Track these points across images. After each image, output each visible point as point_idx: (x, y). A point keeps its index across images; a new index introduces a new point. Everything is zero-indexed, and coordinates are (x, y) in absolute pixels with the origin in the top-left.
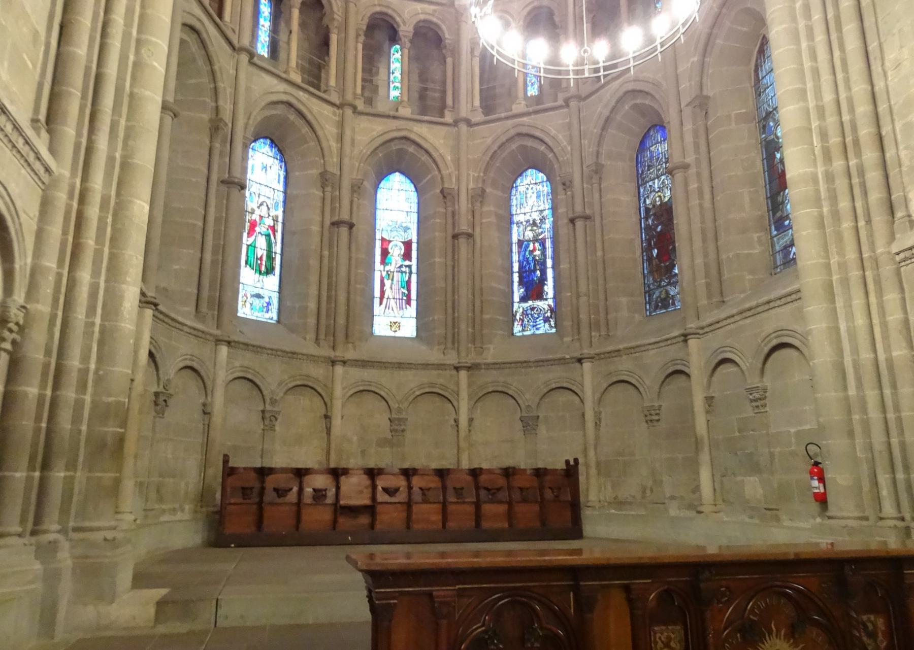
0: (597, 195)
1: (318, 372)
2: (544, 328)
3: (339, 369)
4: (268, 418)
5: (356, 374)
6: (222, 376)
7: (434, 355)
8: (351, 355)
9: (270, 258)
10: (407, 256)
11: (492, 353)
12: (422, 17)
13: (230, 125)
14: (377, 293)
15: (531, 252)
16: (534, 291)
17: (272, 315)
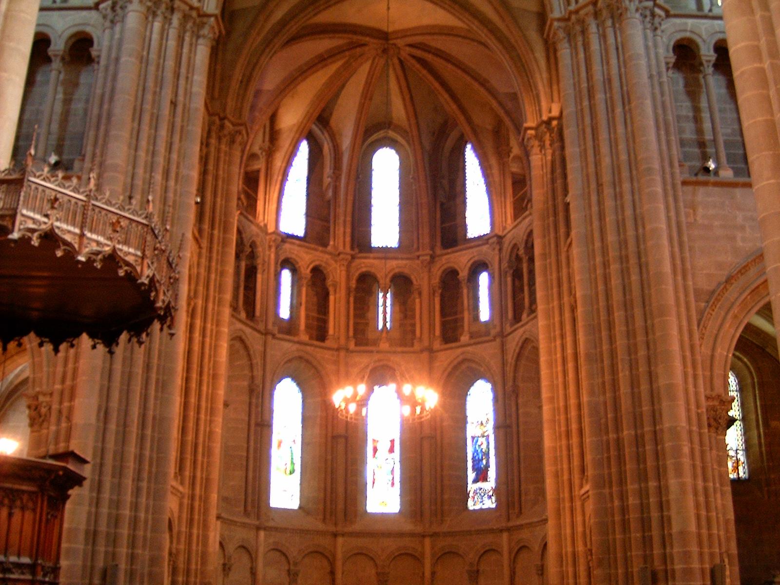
0: (514, 409)
1: (325, 542)
2: (490, 504)
6: (261, 550)
7: (408, 527)
8: (350, 529)
9: (293, 463)
10: (392, 450)
12: (397, 271)
13: (261, 386)
15: (480, 446)
16: (482, 476)
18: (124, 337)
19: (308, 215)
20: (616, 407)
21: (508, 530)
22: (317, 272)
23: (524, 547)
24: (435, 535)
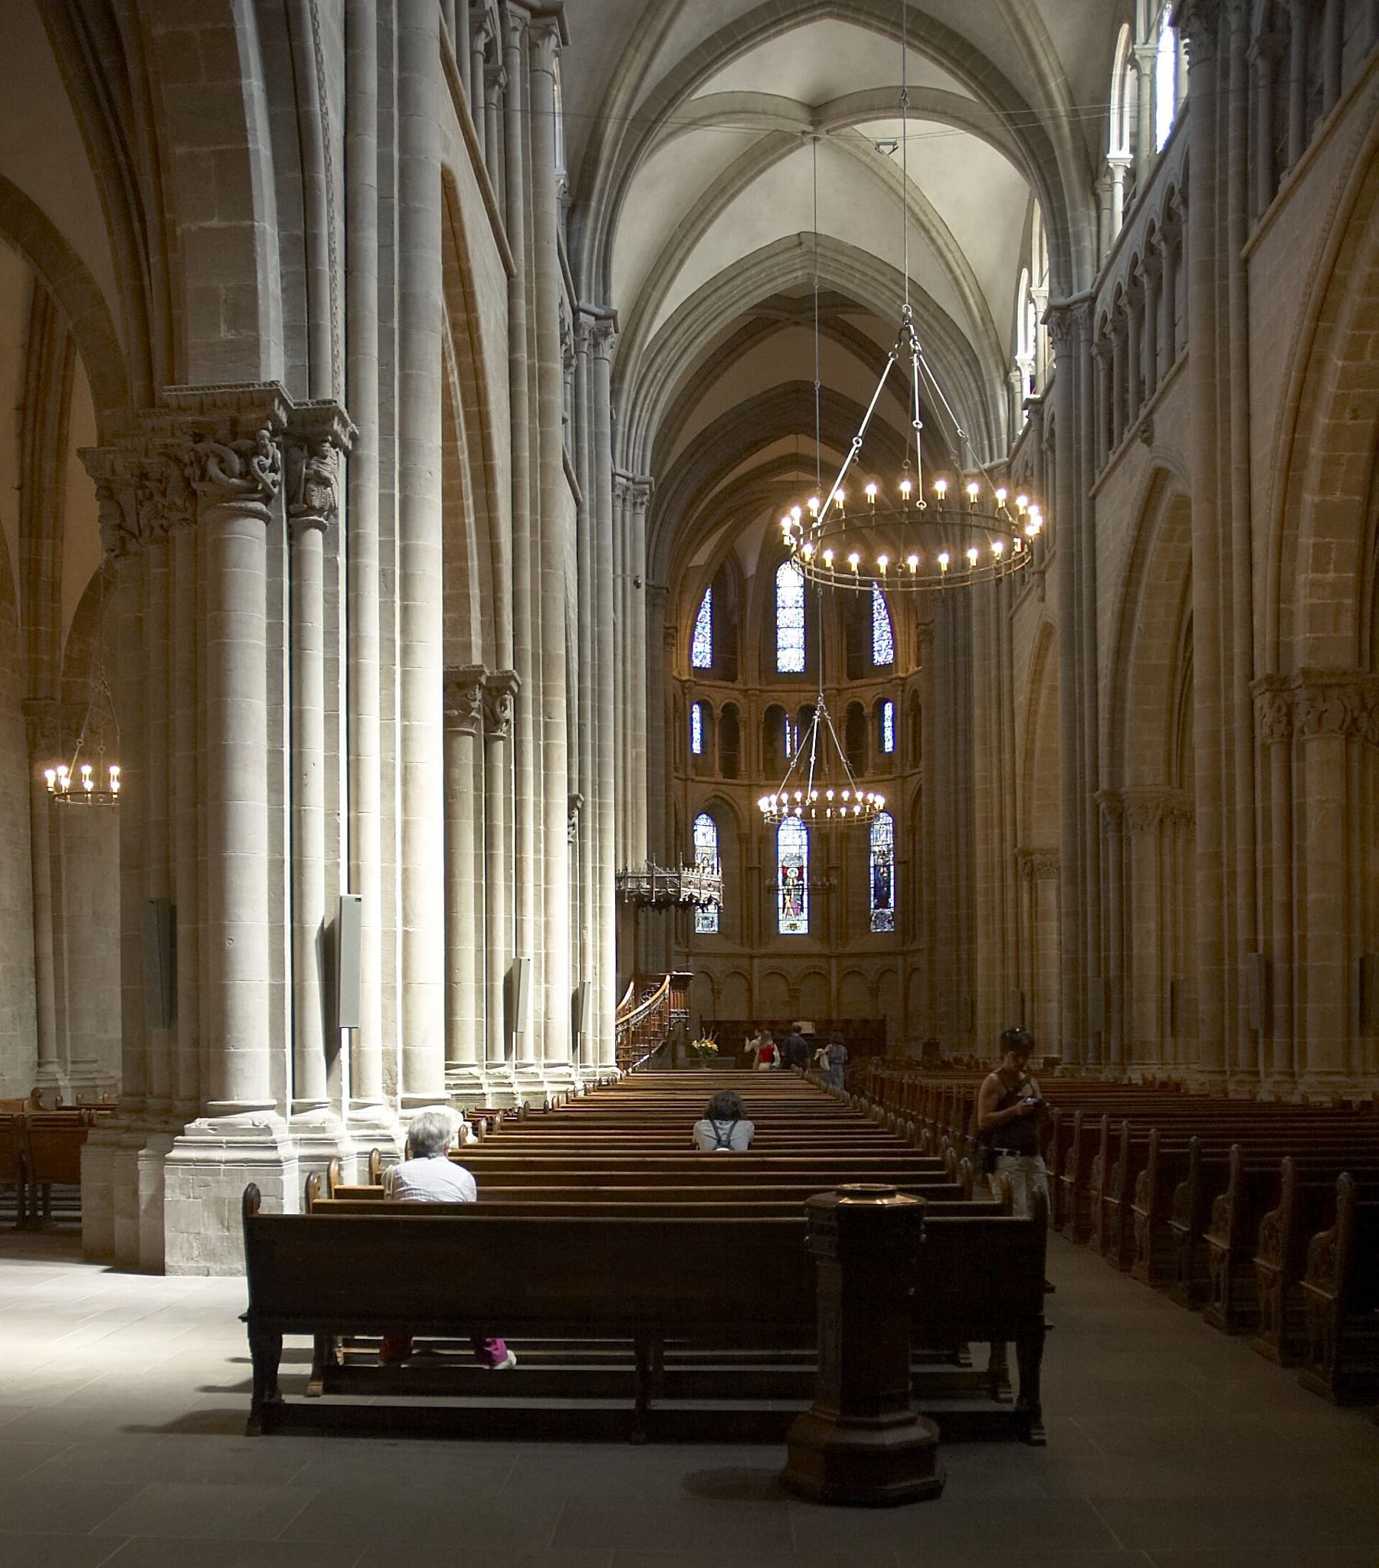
1: (744, 963)
2: (888, 928)
7: (817, 948)
8: (763, 951)
10: (800, 877)
11: (853, 947)
12: (803, 703)
14: (781, 905)
20: (957, 895)
21: (903, 954)
22: (730, 710)
23: (917, 969)
24: (839, 956)
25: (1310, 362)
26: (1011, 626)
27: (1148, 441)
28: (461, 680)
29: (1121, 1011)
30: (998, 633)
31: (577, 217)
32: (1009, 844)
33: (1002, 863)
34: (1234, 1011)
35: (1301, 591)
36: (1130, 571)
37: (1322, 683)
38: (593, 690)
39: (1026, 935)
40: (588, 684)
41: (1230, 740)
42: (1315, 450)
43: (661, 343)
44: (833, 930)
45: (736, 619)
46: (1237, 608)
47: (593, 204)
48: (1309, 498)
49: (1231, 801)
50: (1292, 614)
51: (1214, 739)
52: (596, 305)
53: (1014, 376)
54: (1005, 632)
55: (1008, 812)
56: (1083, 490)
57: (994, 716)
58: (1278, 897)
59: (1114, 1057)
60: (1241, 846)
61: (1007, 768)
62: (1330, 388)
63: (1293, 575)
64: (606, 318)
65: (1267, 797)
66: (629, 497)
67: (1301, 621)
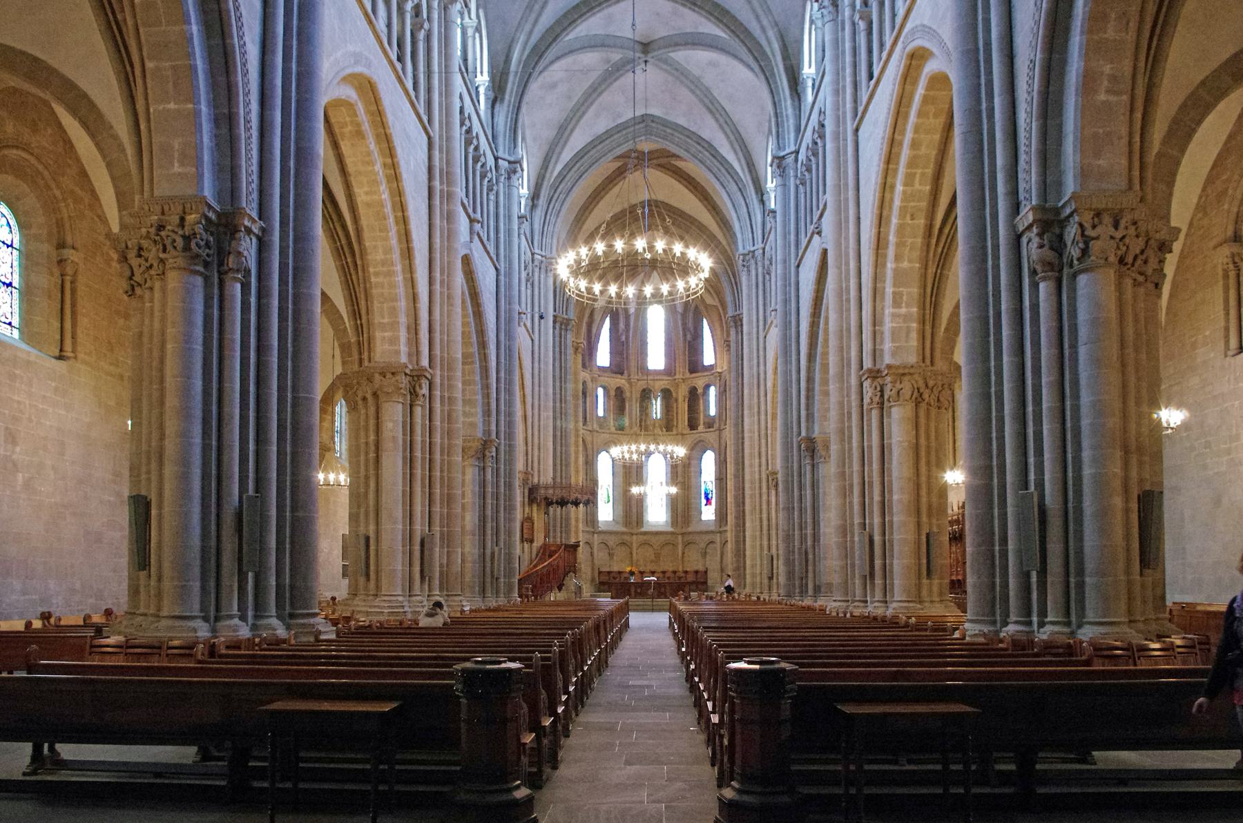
1: (627, 538)
3: (635, 537)
4: (611, 555)
5: (641, 538)
6: (596, 543)
16: (708, 501)
17: (611, 519)
18: (581, 505)
19: (611, 353)
21: (720, 532)
25: (886, 186)
26: (765, 342)
27: (819, 233)
28: (393, 370)
29: (814, 565)
30: (758, 345)
31: (497, 106)
32: (764, 467)
33: (760, 479)
34: (853, 565)
35: (887, 319)
36: (815, 309)
37: (901, 373)
38: (505, 379)
39: (774, 521)
40: (502, 375)
41: (850, 407)
42: (892, 238)
43: (562, 177)
44: (679, 519)
45: (623, 338)
46: (854, 330)
47: (507, 97)
48: (890, 265)
49: (850, 443)
50: (882, 333)
51: (841, 404)
52: (509, 155)
53: (765, 198)
54: (761, 345)
55: (763, 450)
56: (793, 261)
57: (756, 394)
58: (877, 498)
59: (810, 592)
60: (856, 467)
61: (763, 423)
62: (897, 203)
63: (883, 309)
64: (515, 162)
65: (870, 440)
66: (543, 266)
67: (887, 335)
